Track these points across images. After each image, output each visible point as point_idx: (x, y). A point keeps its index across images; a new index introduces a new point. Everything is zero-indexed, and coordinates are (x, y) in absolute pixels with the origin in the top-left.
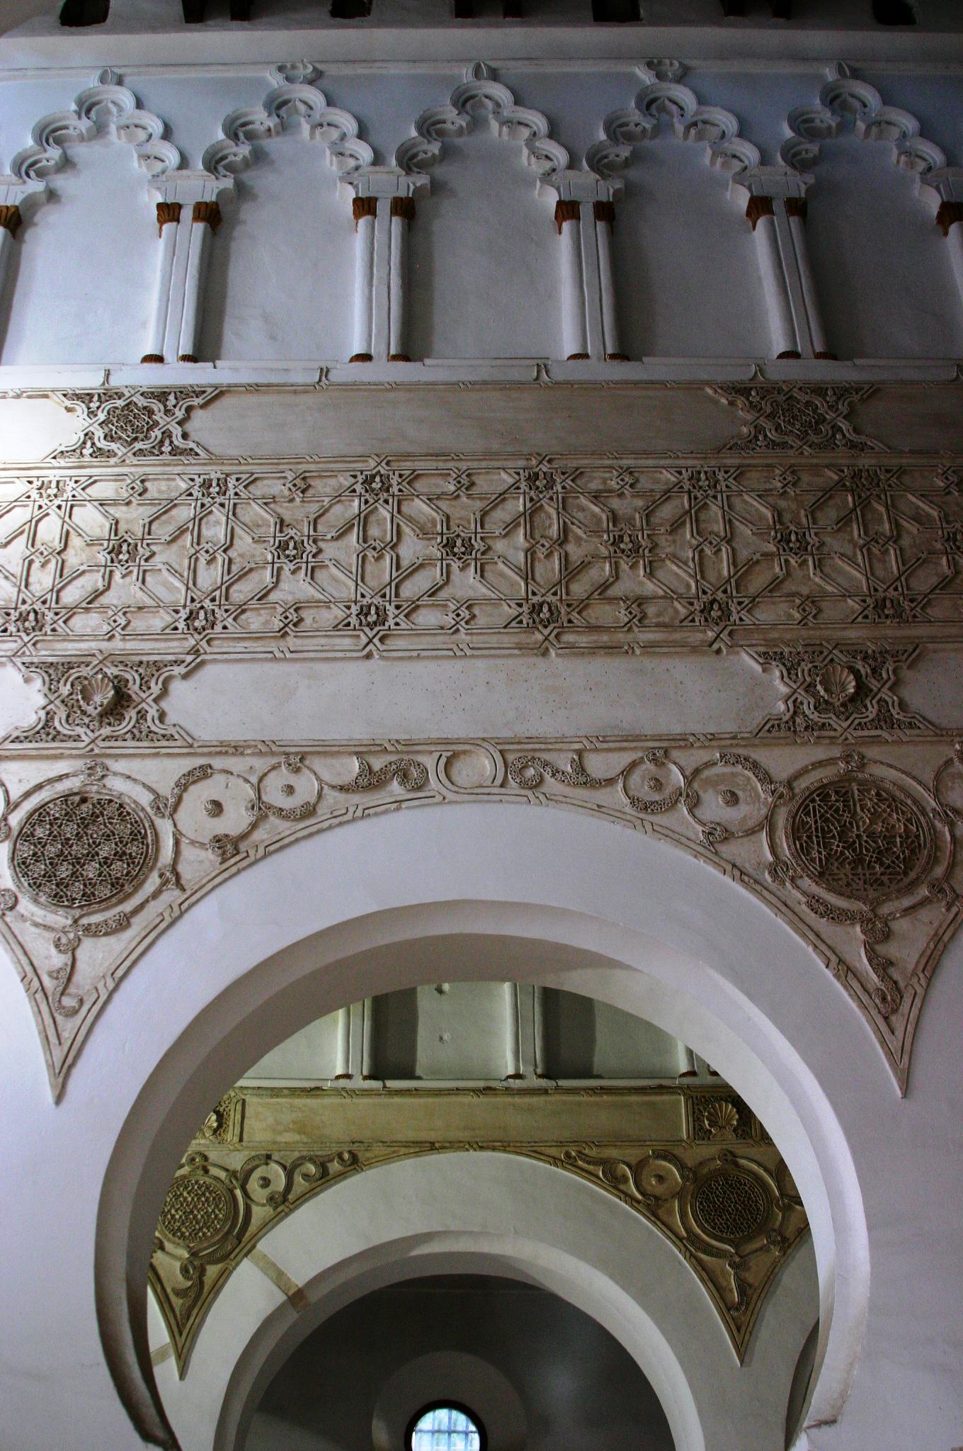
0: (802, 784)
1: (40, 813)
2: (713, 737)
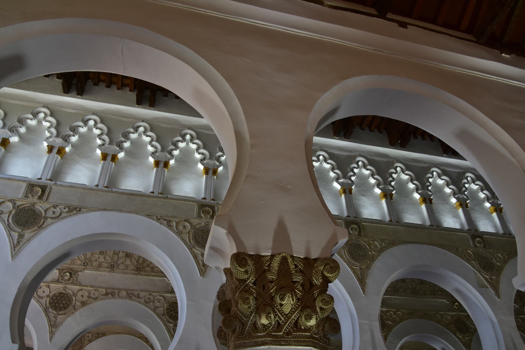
1: (55, 295)
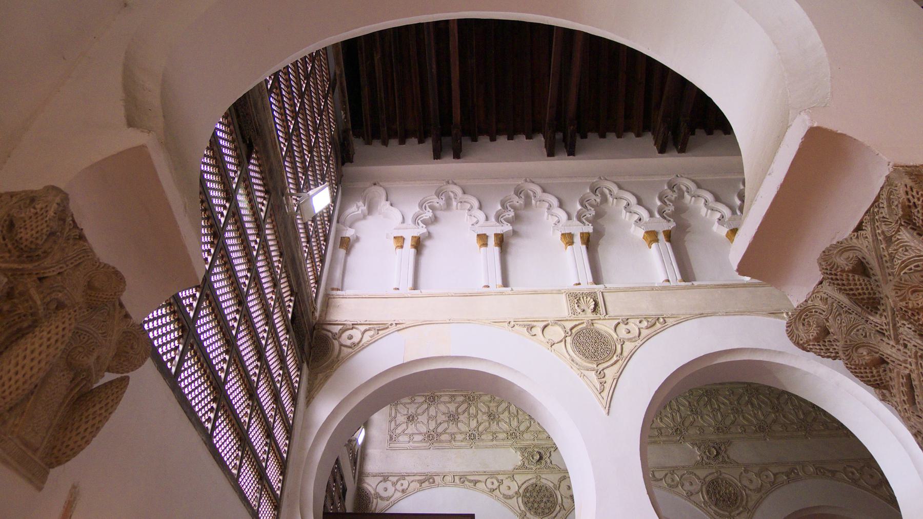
0: (708, 479)
1: (526, 490)
2: (683, 467)
